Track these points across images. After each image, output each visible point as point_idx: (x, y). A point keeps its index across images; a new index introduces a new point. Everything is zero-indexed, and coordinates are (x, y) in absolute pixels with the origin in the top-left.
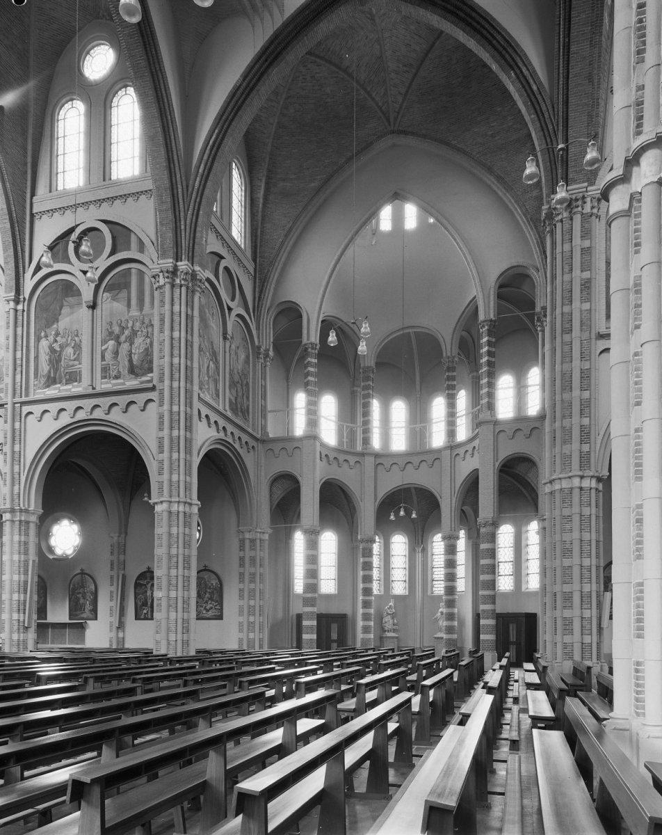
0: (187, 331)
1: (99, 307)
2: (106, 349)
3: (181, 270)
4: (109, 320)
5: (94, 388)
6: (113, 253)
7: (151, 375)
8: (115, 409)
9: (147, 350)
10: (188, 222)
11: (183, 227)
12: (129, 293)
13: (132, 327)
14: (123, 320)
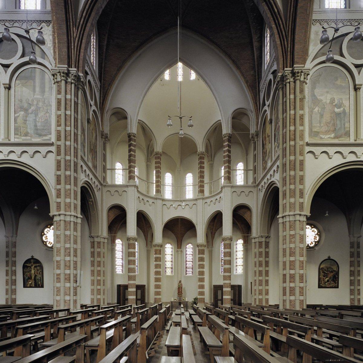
0: (75, 111)
1: (12, 90)
2: (19, 116)
3: (72, 73)
4: (20, 98)
5: (9, 140)
6: (23, 56)
7: (50, 136)
8: (25, 155)
9: (46, 120)
10: (76, 45)
11: (73, 47)
12: (34, 82)
13: (37, 104)
14: (30, 99)
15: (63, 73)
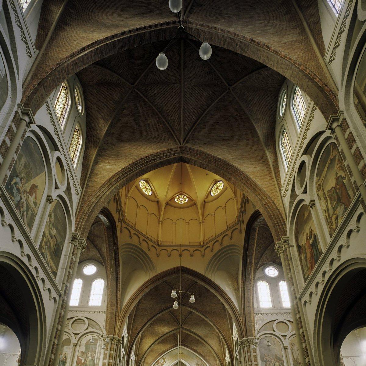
15: (110, 339)
